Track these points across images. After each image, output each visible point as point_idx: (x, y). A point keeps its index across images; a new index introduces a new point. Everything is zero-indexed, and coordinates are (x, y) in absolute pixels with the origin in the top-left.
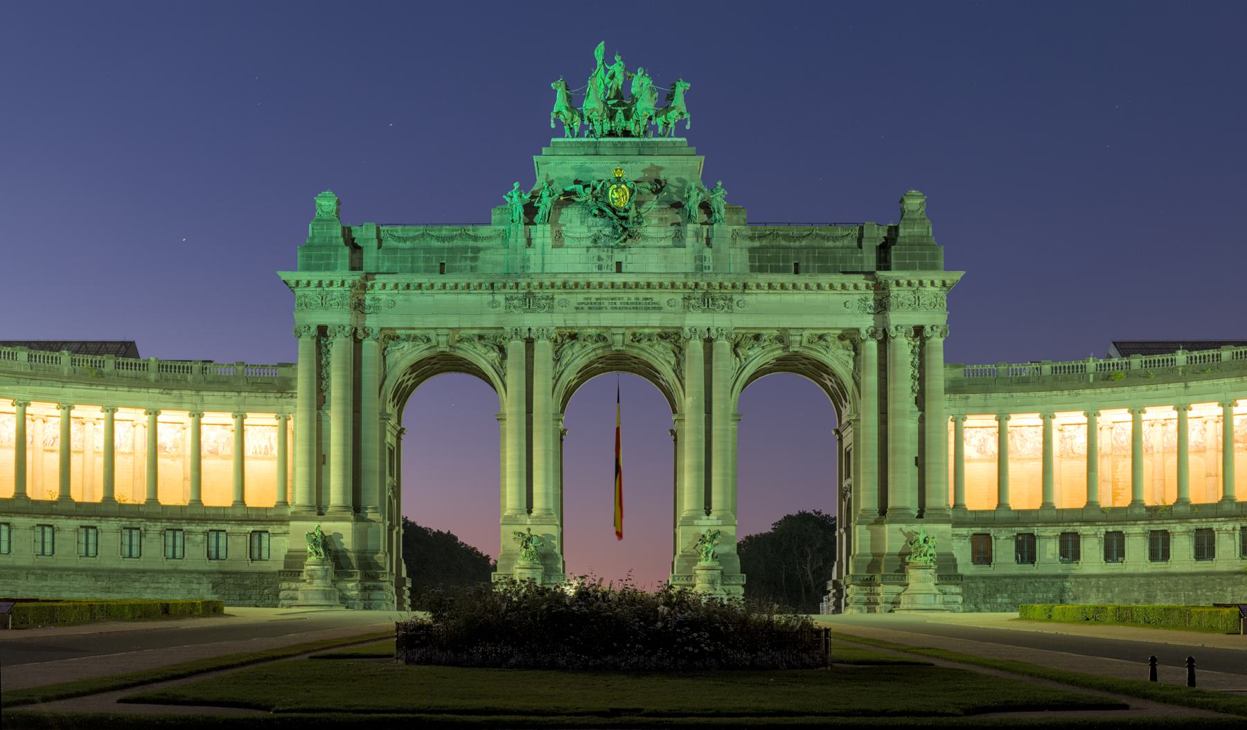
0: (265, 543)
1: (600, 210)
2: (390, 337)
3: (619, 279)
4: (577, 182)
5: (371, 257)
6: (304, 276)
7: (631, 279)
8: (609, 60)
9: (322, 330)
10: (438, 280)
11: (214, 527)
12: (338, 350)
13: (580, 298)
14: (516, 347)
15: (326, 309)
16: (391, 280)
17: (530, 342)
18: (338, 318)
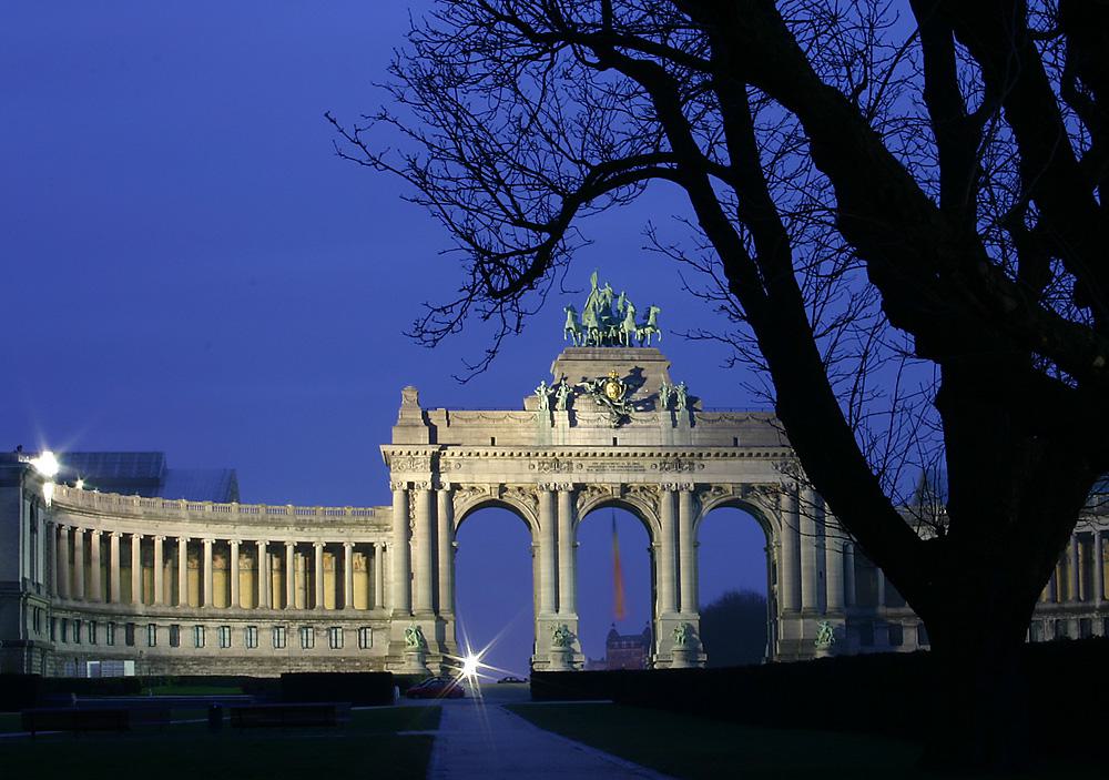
0: (369, 636)
1: (601, 400)
2: (456, 487)
3: (615, 451)
4: (584, 379)
5: (444, 435)
6: (398, 449)
7: (624, 451)
8: (600, 285)
9: (411, 485)
10: (491, 451)
11: (334, 625)
12: (420, 500)
13: (590, 463)
14: (544, 497)
15: (414, 470)
16: (457, 451)
17: (554, 494)
18: (423, 477)
